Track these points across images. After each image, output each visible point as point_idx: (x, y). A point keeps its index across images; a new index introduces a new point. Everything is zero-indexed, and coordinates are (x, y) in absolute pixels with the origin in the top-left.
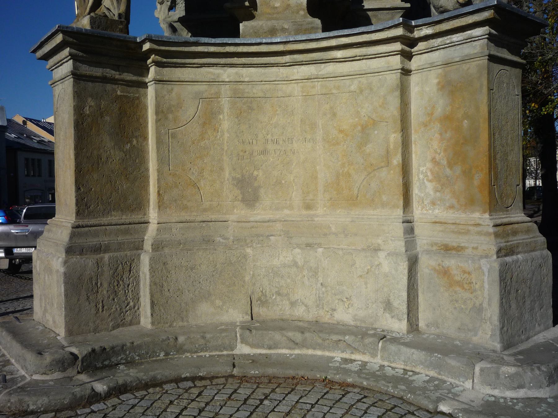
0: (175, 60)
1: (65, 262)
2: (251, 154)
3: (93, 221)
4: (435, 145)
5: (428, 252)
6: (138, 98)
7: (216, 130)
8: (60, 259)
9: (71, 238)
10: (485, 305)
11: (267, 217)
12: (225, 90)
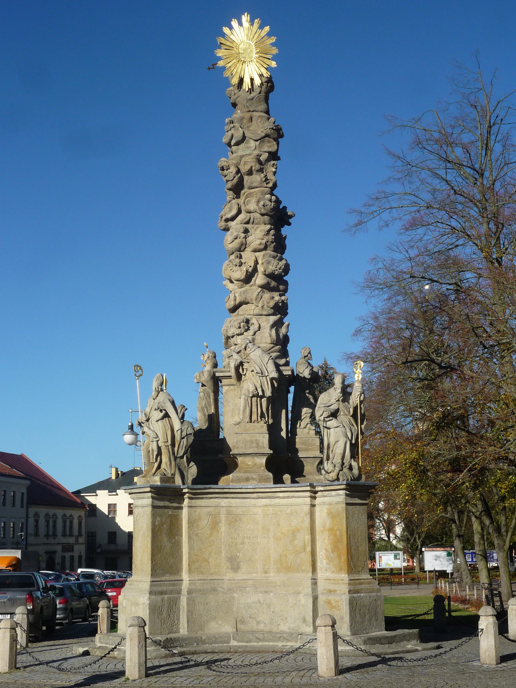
0: (198, 496)
1: (149, 598)
2: (236, 544)
3: (158, 579)
4: (326, 541)
5: (322, 593)
6: (178, 515)
7: (218, 532)
8: (146, 598)
9: (150, 587)
10: (344, 616)
11: (244, 578)
12: (223, 511)
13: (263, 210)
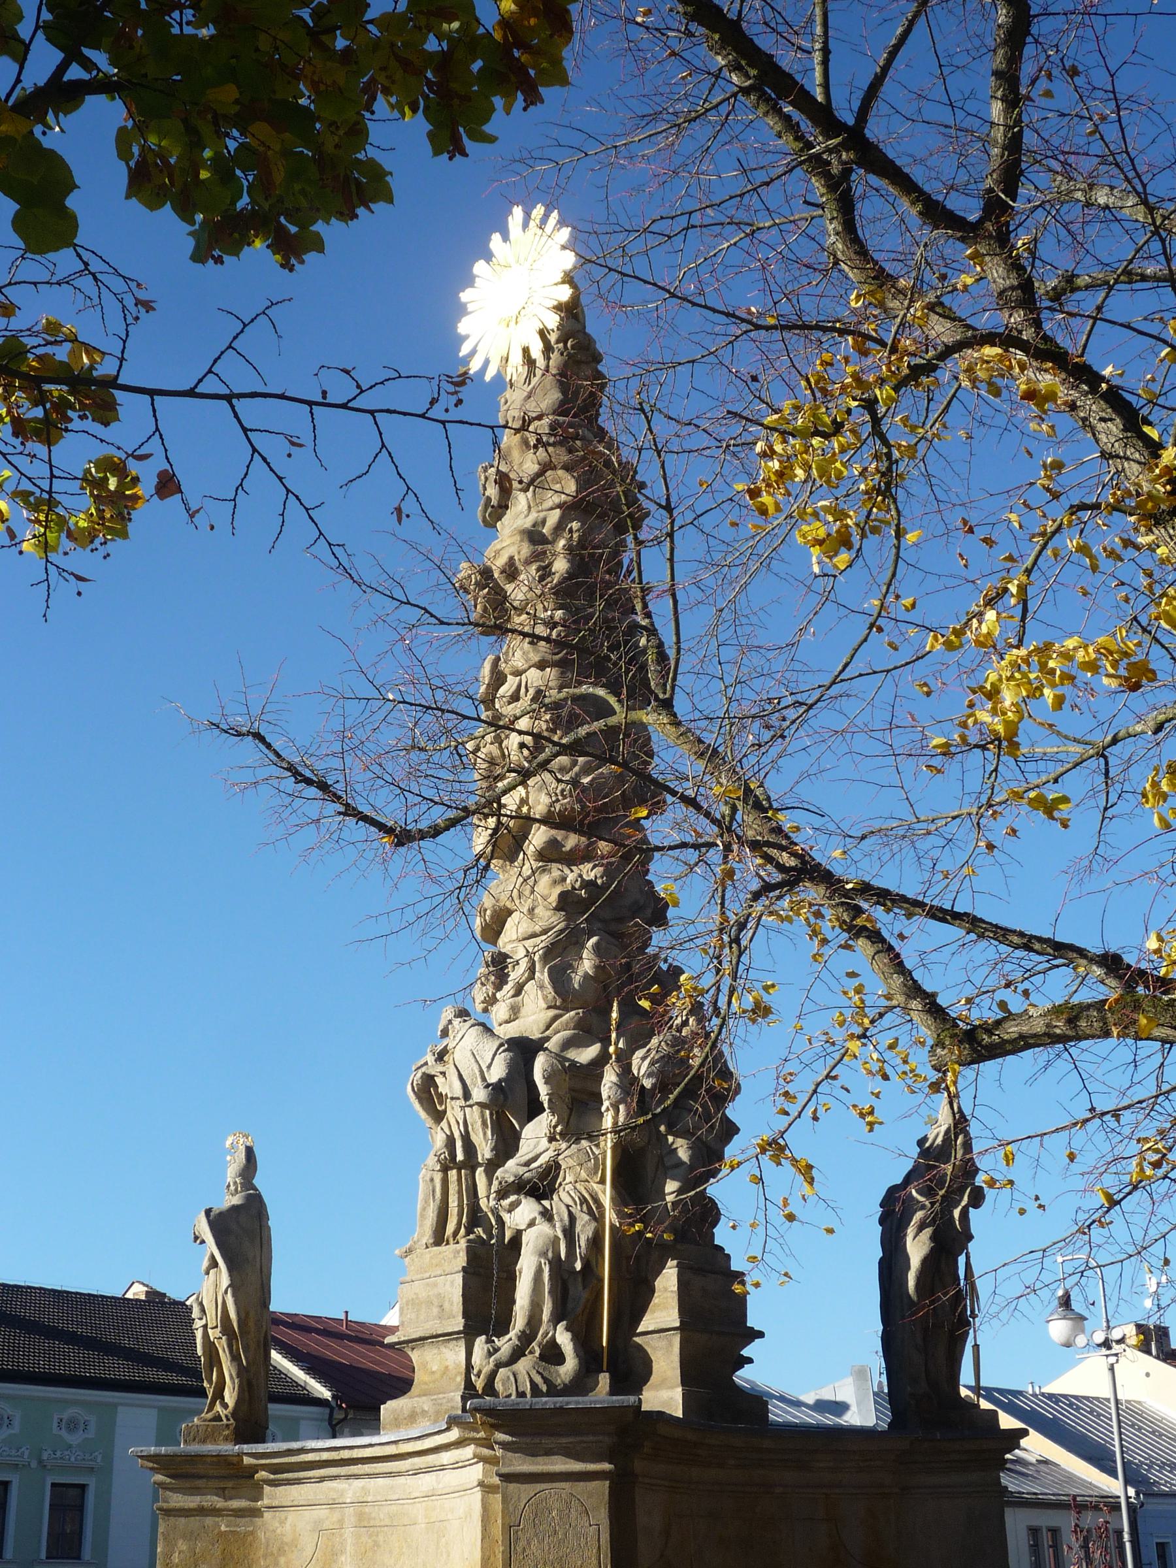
0: (285, 1476)
6: (252, 1533)
13: (531, 655)
